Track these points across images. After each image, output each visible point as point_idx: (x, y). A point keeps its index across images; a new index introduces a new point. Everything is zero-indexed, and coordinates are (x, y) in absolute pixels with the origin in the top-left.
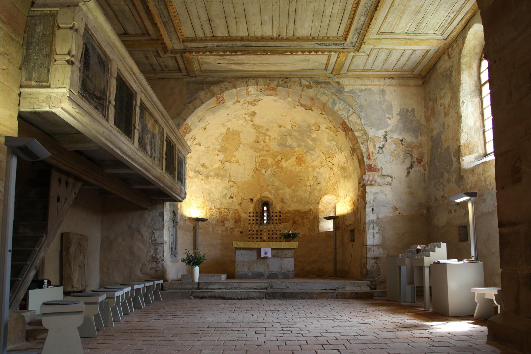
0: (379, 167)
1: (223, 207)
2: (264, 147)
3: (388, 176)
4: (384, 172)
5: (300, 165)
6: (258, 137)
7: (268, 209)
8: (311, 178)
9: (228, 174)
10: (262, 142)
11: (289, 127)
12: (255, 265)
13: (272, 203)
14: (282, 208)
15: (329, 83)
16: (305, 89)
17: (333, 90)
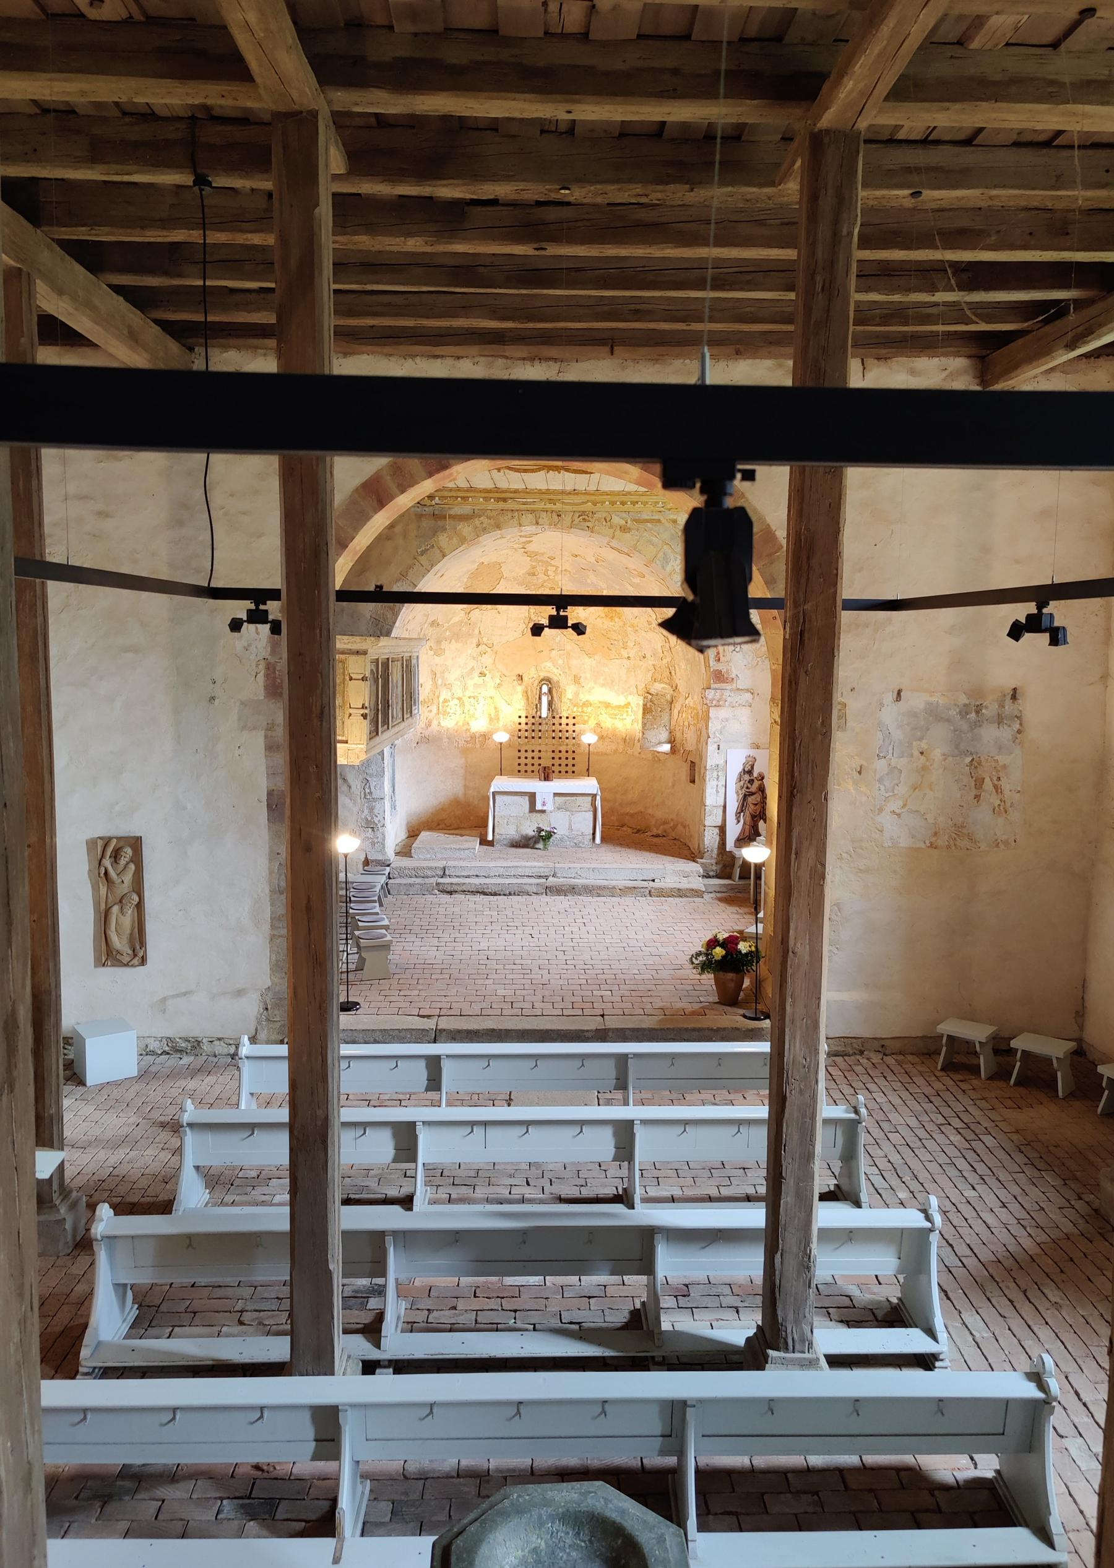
0: (733, 676)
1: (468, 694)
2: (545, 582)
3: (748, 690)
4: (741, 684)
5: (612, 619)
6: (533, 567)
7: (550, 691)
8: (630, 644)
9: (477, 631)
10: (541, 575)
11: (593, 560)
12: (528, 823)
13: (558, 682)
14: (577, 694)
15: (659, 521)
16: (618, 532)
17: (666, 536)
